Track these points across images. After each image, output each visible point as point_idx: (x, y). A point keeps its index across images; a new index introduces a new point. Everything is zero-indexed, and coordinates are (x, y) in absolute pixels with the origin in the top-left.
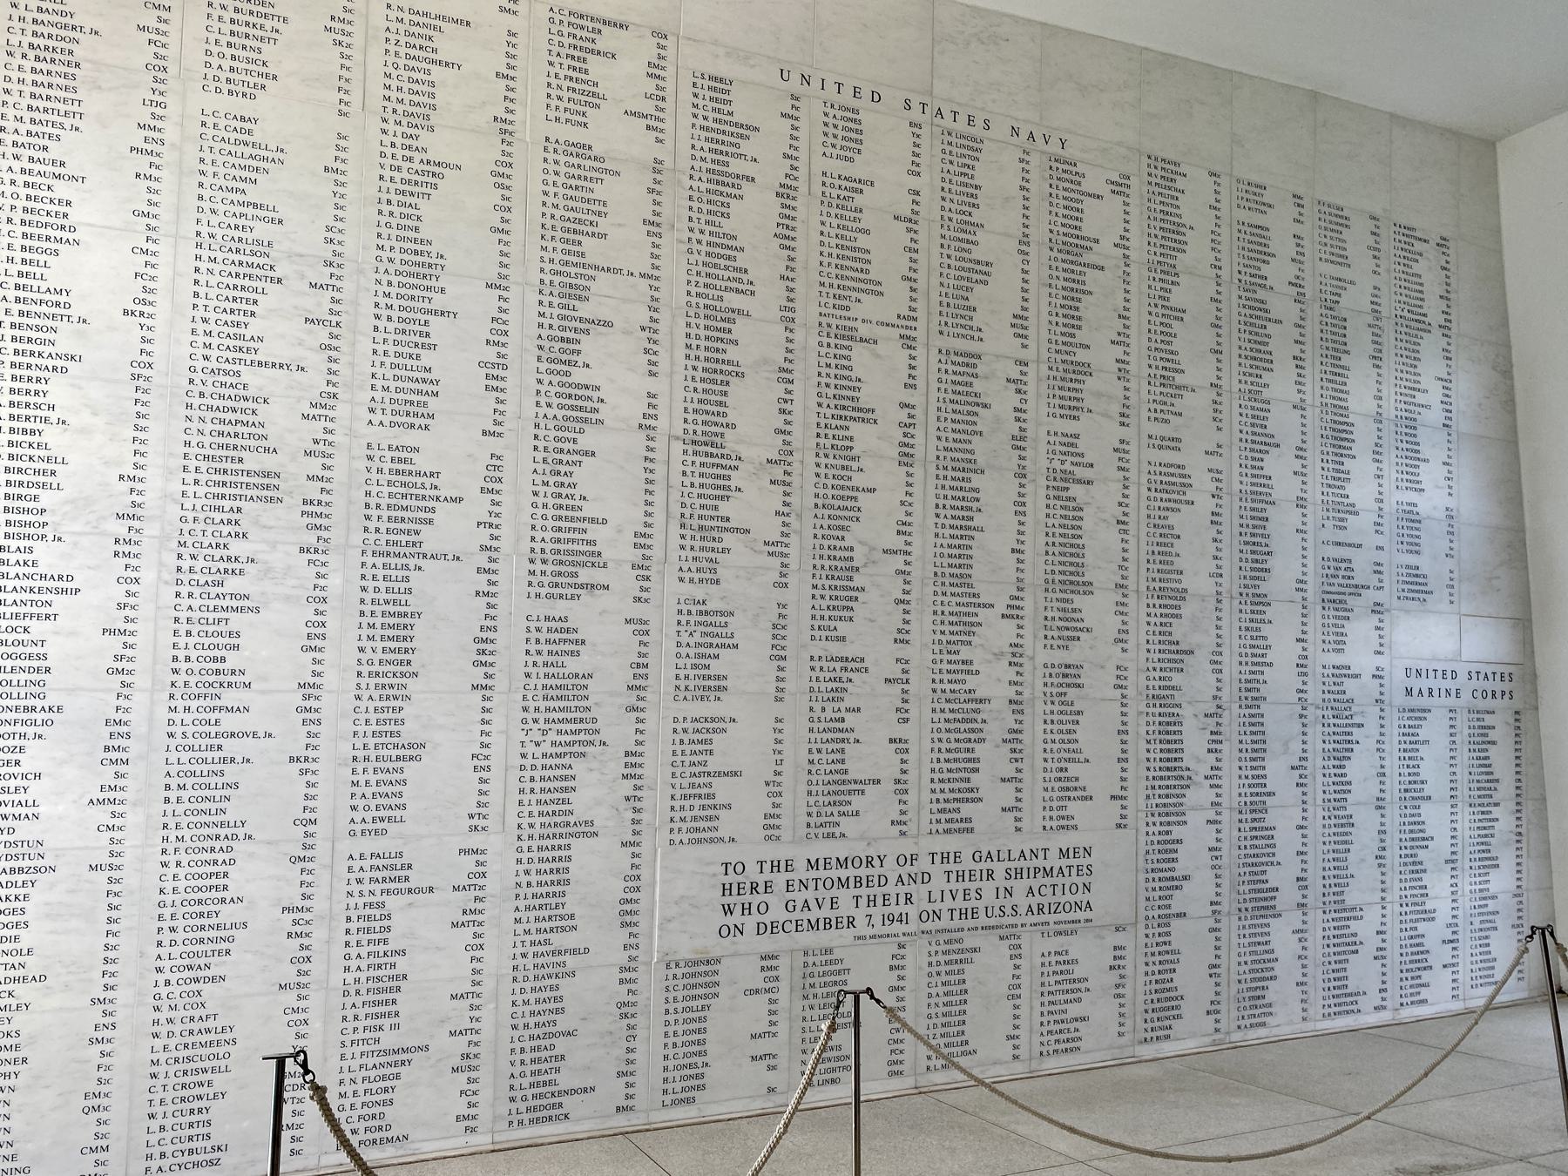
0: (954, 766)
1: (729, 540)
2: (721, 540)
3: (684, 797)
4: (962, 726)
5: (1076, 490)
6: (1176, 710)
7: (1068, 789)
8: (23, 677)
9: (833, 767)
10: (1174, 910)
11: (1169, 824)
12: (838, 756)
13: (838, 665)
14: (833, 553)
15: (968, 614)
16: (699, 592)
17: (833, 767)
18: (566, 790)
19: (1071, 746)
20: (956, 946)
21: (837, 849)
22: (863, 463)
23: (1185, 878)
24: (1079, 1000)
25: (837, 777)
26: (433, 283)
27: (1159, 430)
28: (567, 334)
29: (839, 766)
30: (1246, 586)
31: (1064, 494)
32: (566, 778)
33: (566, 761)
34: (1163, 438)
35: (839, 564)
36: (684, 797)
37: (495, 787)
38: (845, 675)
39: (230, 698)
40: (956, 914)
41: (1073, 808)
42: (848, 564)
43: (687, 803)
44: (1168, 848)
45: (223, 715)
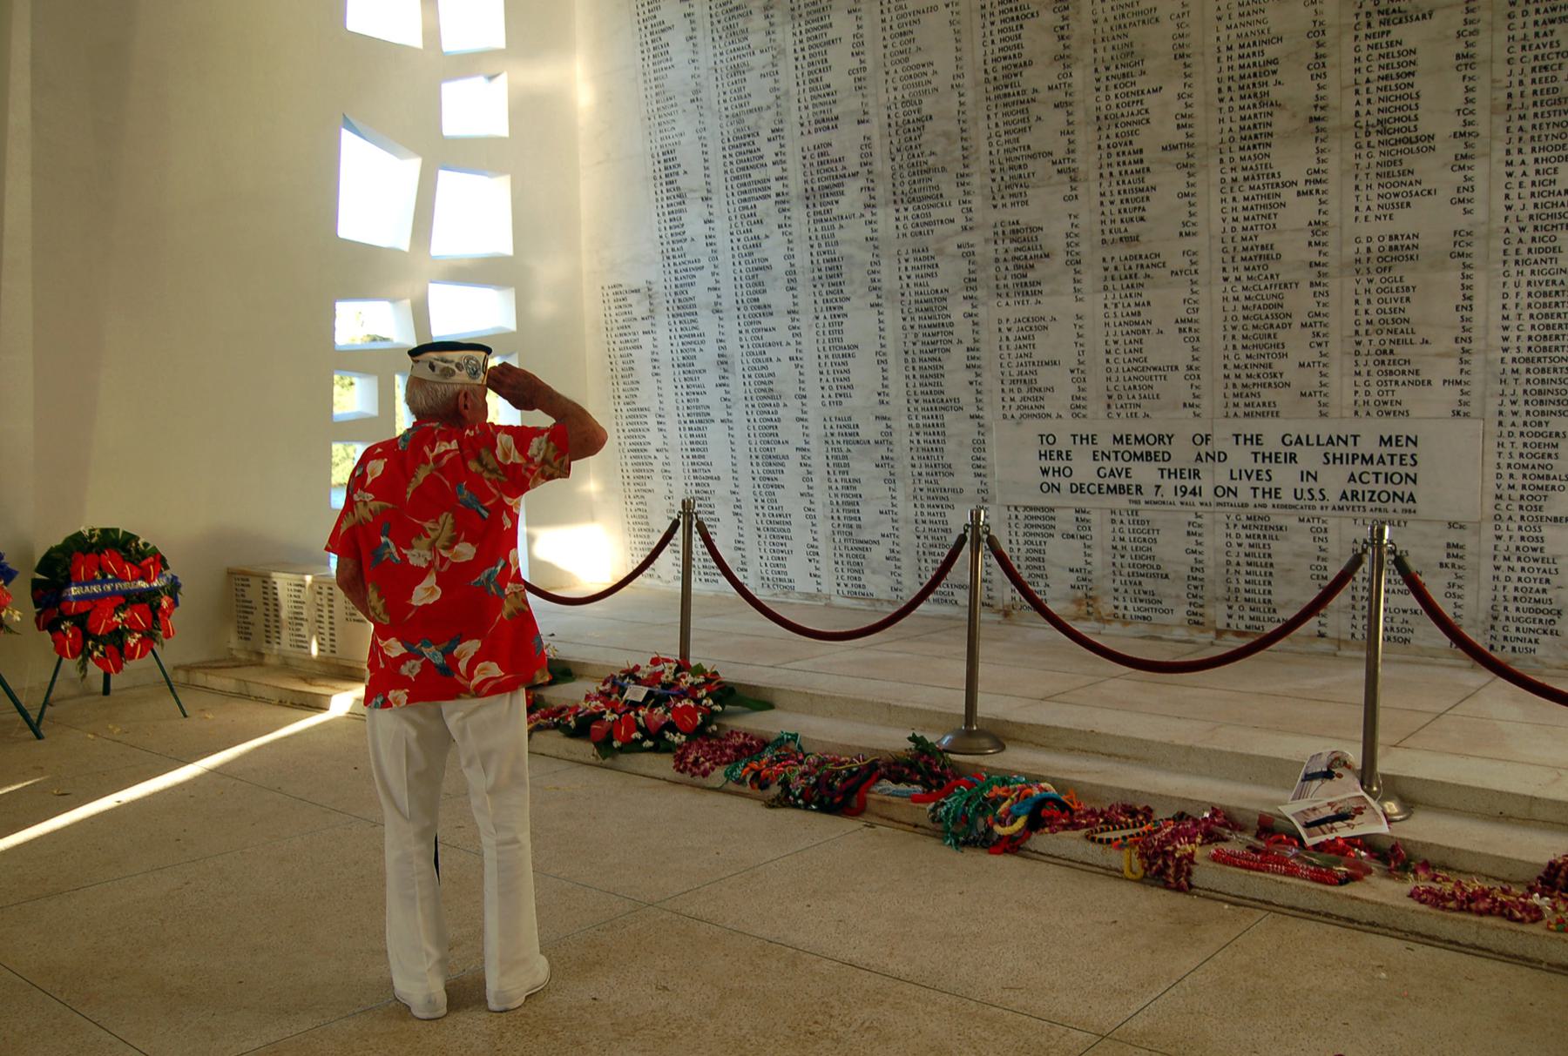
0: (1254, 352)
1: (1032, 165)
2: (1026, 166)
3: (1013, 382)
4: (1263, 313)
5: (1397, 32)
6: (1558, 278)
7: (1391, 373)
8: (688, 318)
9: (1131, 356)
11: (1543, 413)
12: (1137, 346)
13: (1133, 264)
14: (1121, 159)
15: (1268, 196)
16: (1009, 214)
17: (1131, 356)
18: (937, 376)
19: (1400, 327)
20: (1259, 523)
21: (1141, 428)
22: (1148, 65)
25: (1135, 365)
26: (827, 21)
28: (906, 29)
29: (1137, 355)
31: (1384, 40)
32: (936, 368)
33: (936, 355)
35: (1129, 168)
36: (1013, 382)
37: (891, 374)
38: (1141, 273)
39: (766, 322)
40: (1259, 493)
41: (1401, 393)
42: (1139, 167)
43: (1015, 387)
45: (765, 334)
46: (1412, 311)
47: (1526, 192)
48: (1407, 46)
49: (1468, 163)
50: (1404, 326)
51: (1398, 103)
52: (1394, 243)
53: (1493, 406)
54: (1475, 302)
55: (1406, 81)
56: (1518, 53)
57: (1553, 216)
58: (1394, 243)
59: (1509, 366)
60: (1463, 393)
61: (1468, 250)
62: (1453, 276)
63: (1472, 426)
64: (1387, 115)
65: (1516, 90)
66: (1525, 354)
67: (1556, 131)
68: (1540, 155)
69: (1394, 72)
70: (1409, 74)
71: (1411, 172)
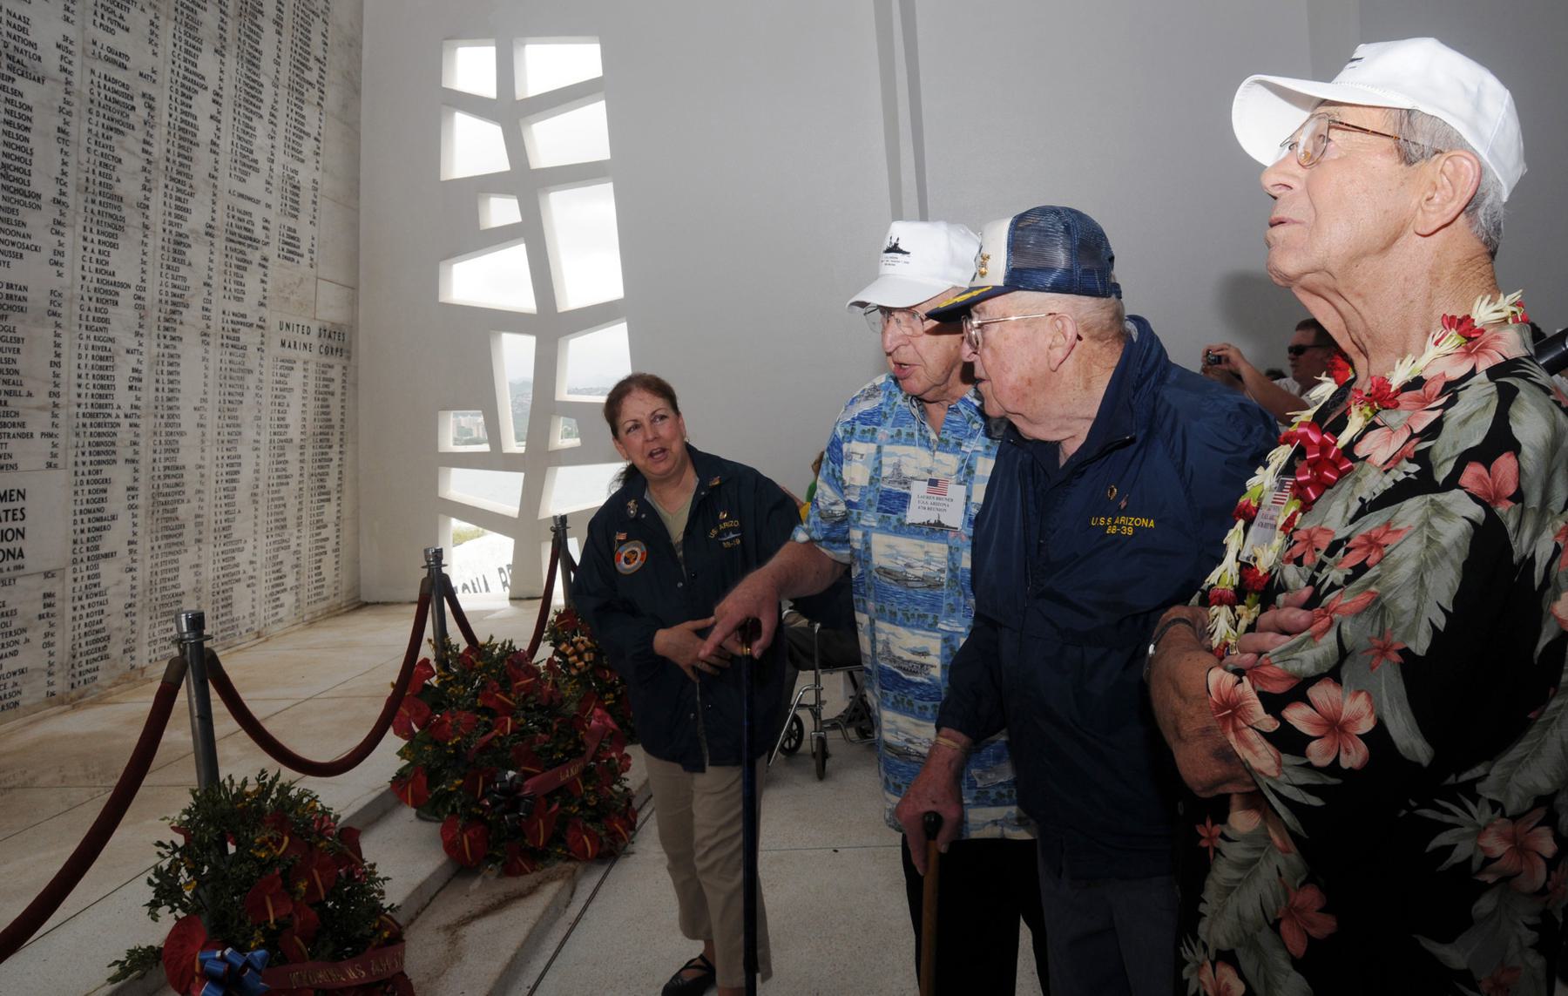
5: (21, 84)
10: (102, 551)
11: (99, 463)
23: (113, 518)
24: (14, 654)
27: (106, 39)
30: (171, 224)
34: (110, 50)
44: (101, 487)
46: (22, 363)
47: (94, 266)
48: (28, 99)
49: (62, 230)
50: (14, 377)
51: (18, 153)
52: (10, 292)
53: (71, 460)
54: (63, 360)
55: (25, 134)
56: (93, 147)
57: (106, 292)
58: (10, 292)
59: (81, 420)
60: (55, 446)
61: (59, 310)
62: (49, 332)
63: (62, 477)
64: (9, 162)
65: (91, 177)
66: (90, 410)
67: (110, 221)
68: (103, 238)
69: (16, 121)
70: (27, 129)
71: (24, 224)
